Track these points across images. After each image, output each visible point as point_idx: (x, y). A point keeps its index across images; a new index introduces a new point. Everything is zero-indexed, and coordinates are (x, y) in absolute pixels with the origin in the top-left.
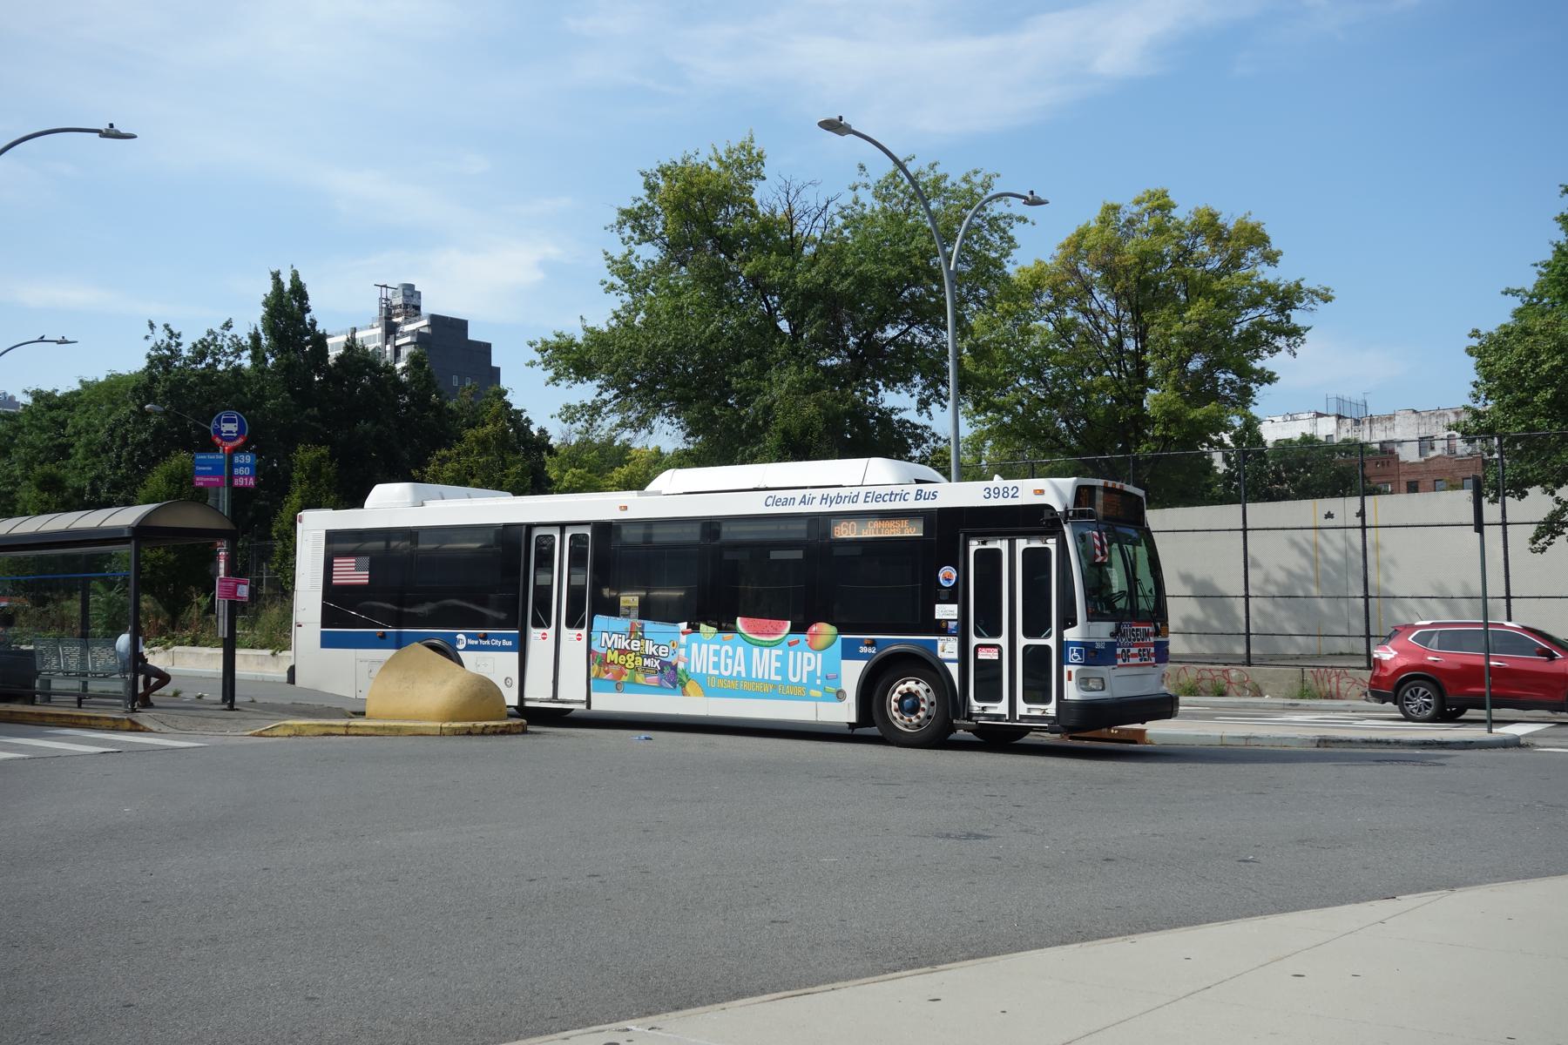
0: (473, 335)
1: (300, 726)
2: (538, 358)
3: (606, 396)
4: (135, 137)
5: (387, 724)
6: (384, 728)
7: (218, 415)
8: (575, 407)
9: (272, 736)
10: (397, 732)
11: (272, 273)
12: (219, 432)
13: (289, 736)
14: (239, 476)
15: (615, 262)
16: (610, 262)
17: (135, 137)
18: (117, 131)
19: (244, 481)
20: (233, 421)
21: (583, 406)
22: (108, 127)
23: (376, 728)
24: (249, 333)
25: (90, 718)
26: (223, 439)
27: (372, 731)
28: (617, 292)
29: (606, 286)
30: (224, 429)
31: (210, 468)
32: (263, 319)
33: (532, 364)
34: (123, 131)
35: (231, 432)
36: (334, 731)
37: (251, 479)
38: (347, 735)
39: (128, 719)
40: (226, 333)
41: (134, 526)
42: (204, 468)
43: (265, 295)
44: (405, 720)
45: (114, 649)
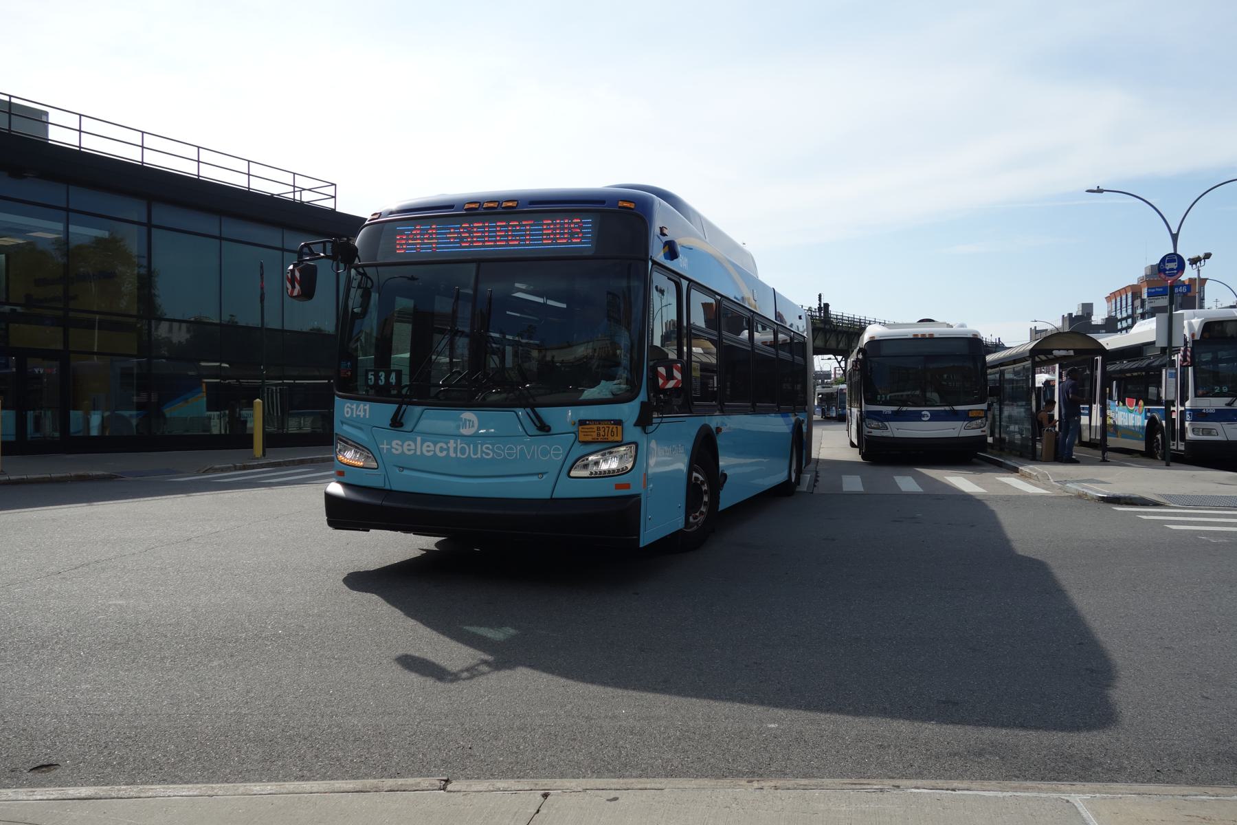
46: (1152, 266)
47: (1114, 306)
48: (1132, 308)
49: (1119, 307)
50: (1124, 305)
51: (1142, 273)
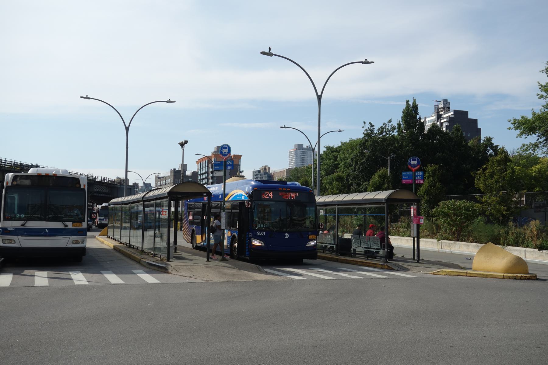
0: (470, 116)
1: (448, 272)
2: (512, 126)
3: (541, 140)
4: (374, 62)
5: (482, 273)
6: (481, 274)
7: (410, 159)
8: (527, 145)
9: (438, 275)
10: (486, 276)
11: (406, 101)
12: (410, 164)
13: (445, 275)
14: (418, 179)
15: (542, 86)
16: (540, 86)
17: (374, 62)
18: (368, 61)
20: (415, 160)
21: (531, 144)
22: (365, 60)
23: (478, 274)
24: (397, 123)
25: (373, 264)
27: (476, 275)
28: (544, 98)
29: (539, 96)
30: (412, 163)
31: (408, 177)
32: (402, 118)
33: (510, 129)
34: (370, 61)
36: (461, 274)
37: (422, 180)
38: (466, 276)
39: (386, 265)
40: (389, 124)
41: (386, 198)
42: (406, 177)
43: (404, 109)
44: (488, 272)
46: (218, 147)
47: (200, 166)
48: (208, 168)
49: (202, 167)
50: (204, 167)
51: (213, 150)
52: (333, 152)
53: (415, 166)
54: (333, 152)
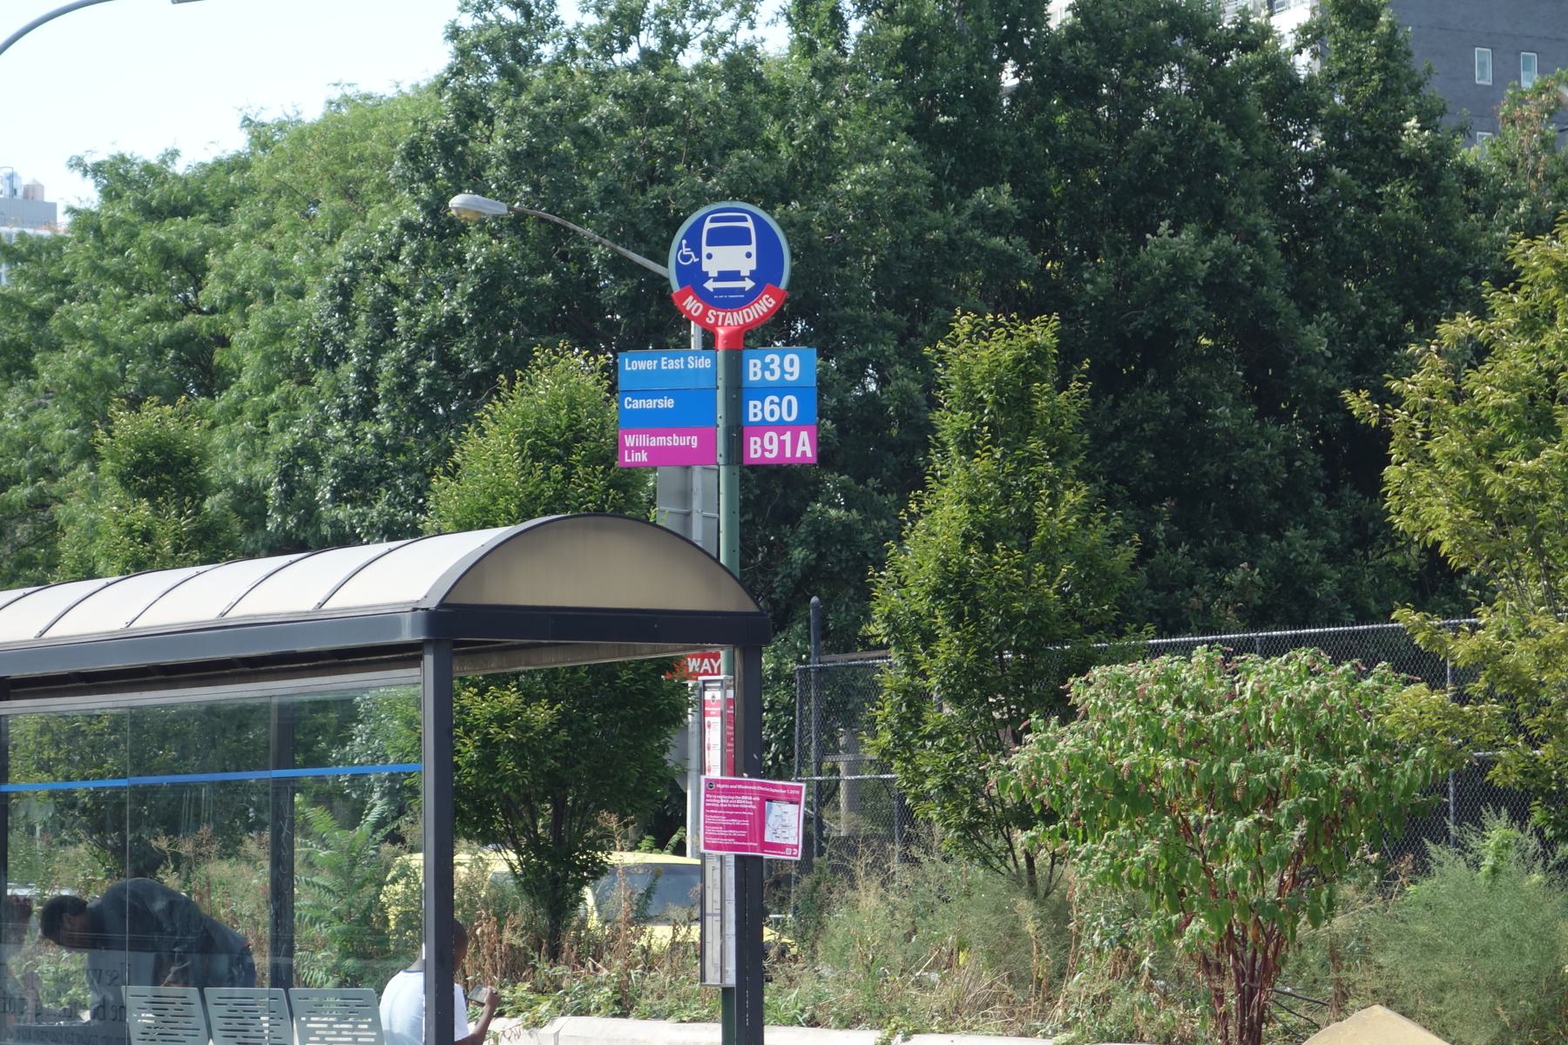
12: (693, 276)
19: (782, 444)
20: (740, 237)
26: (709, 299)
30: (711, 267)
31: (669, 403)
35: (735, 276)
37: (804, 435)
42: (650, 404)
45: (376, 1024)
52: (155, 213)
53: (741, 290)
54: (155, 213)
